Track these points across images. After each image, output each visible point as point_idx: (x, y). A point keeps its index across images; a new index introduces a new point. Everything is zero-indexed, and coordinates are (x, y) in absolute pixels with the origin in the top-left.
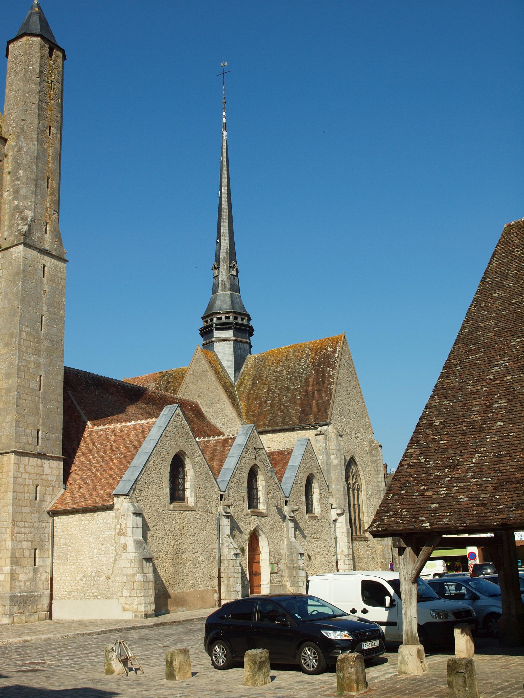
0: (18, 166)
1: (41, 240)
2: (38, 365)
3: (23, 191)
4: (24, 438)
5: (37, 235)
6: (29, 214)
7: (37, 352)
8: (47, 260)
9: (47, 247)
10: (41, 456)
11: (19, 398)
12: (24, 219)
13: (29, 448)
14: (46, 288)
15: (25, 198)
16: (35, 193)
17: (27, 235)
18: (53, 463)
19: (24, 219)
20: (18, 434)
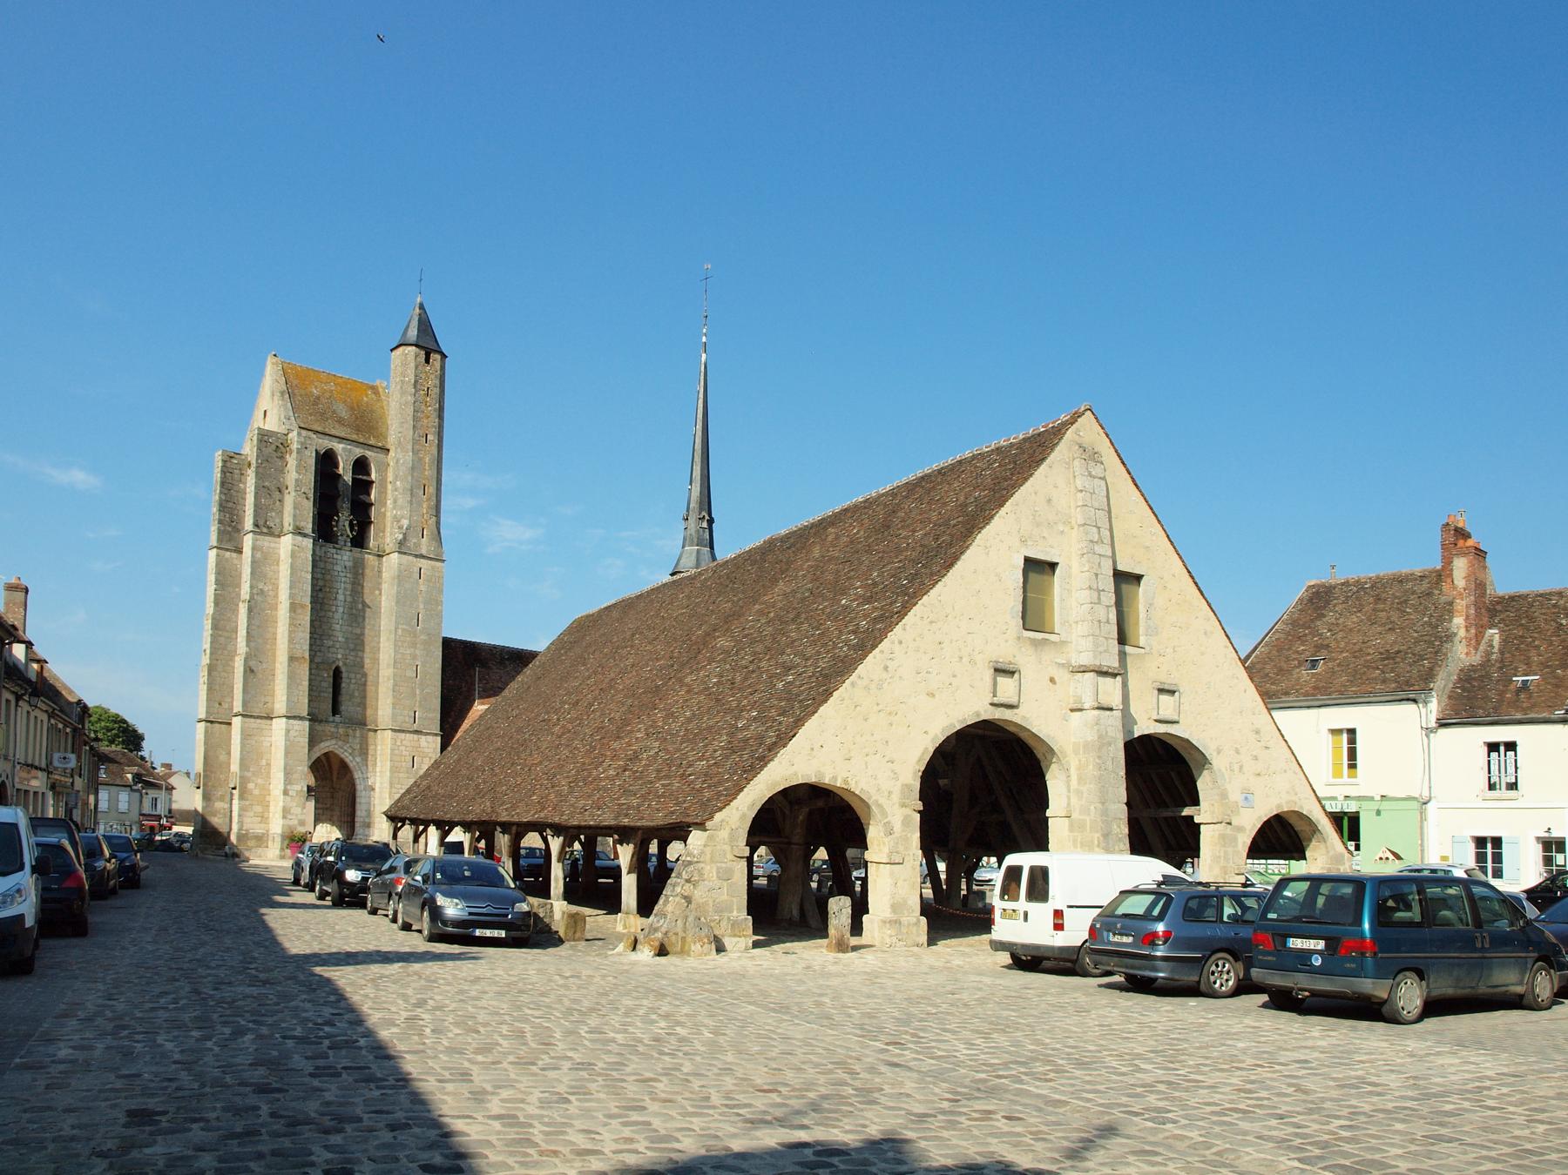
0: (396, 477)
1: (418, 545)
2: (414, 657)
3: (400, 502)
4: (400, 718)
5: (412, 541)
6: (405, 523)
7: (414, 645)
8: (423, 563)
9: (424, 552)
10: (416, 732)
11: (395, 685)
12: (400, 528)
13: (406, 726)
14: (423, 588)
15: (402, 508)
16: (411, 502)
17: (401, 543)
18: (430, 738)
19: (400, 528)
20: (394, 716)
